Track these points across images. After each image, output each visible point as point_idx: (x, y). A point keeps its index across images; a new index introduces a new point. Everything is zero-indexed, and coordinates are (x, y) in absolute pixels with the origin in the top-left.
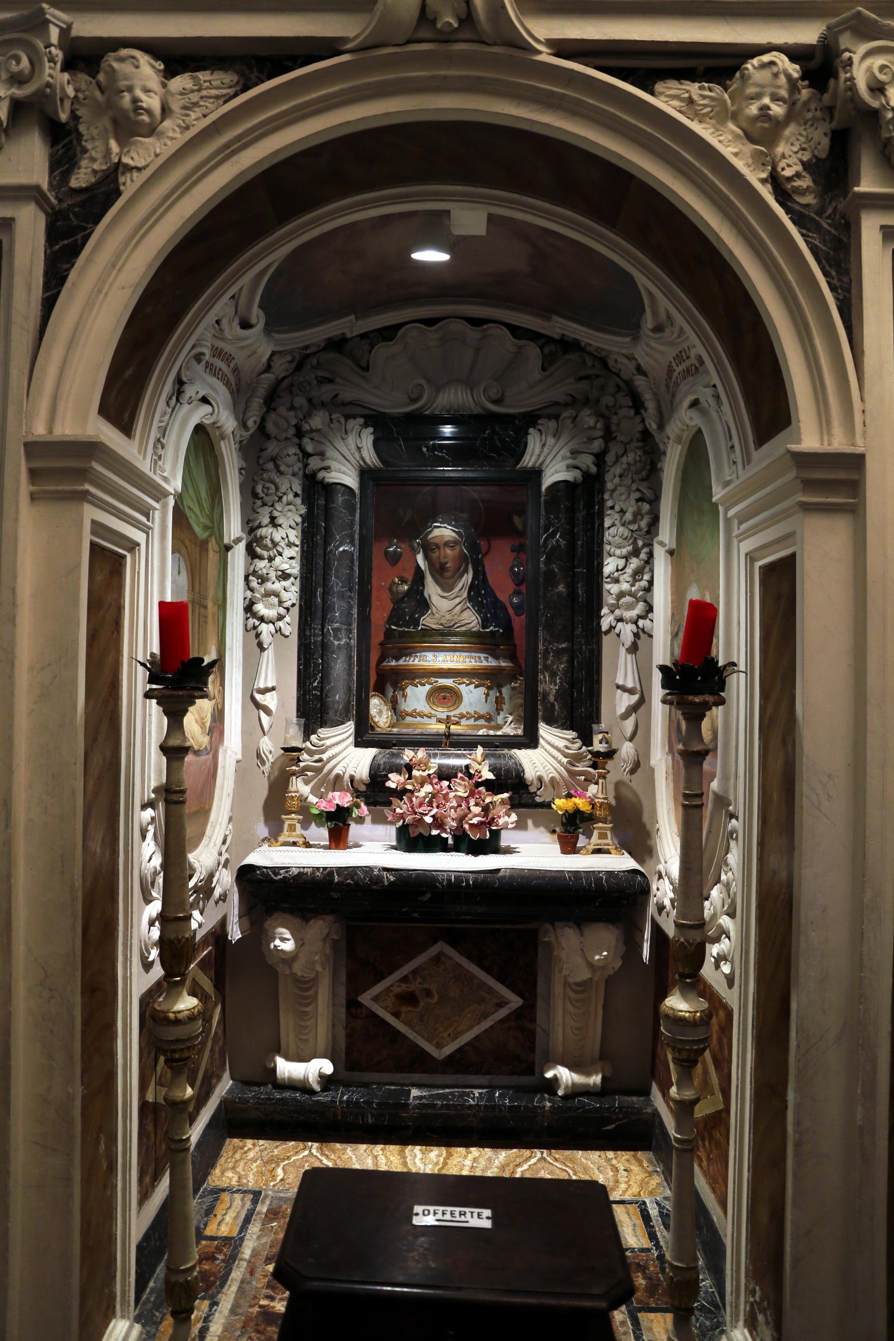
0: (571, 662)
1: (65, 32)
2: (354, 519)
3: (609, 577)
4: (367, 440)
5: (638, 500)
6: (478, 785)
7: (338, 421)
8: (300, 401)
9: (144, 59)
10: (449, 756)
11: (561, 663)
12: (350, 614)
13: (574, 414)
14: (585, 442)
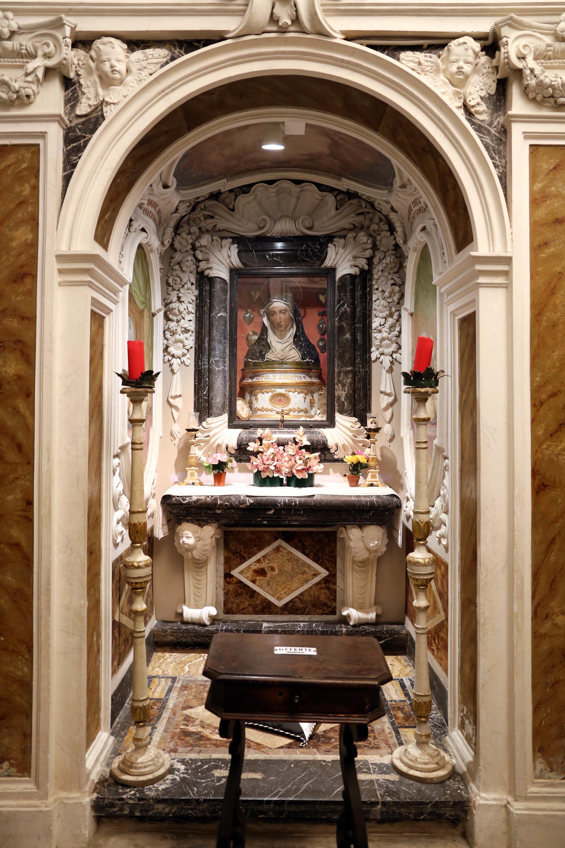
0: (354, 378)
1: (73, 29)
3: (375, 329)
4: (235, 250)
5: (392, 285)
6: (301, 448)
7: (217, 241)
8: (194, 229)
9: (117, 43)
10: (283, 433)
11: (348, 379)
12: (224, 352)
13: (355, 235)
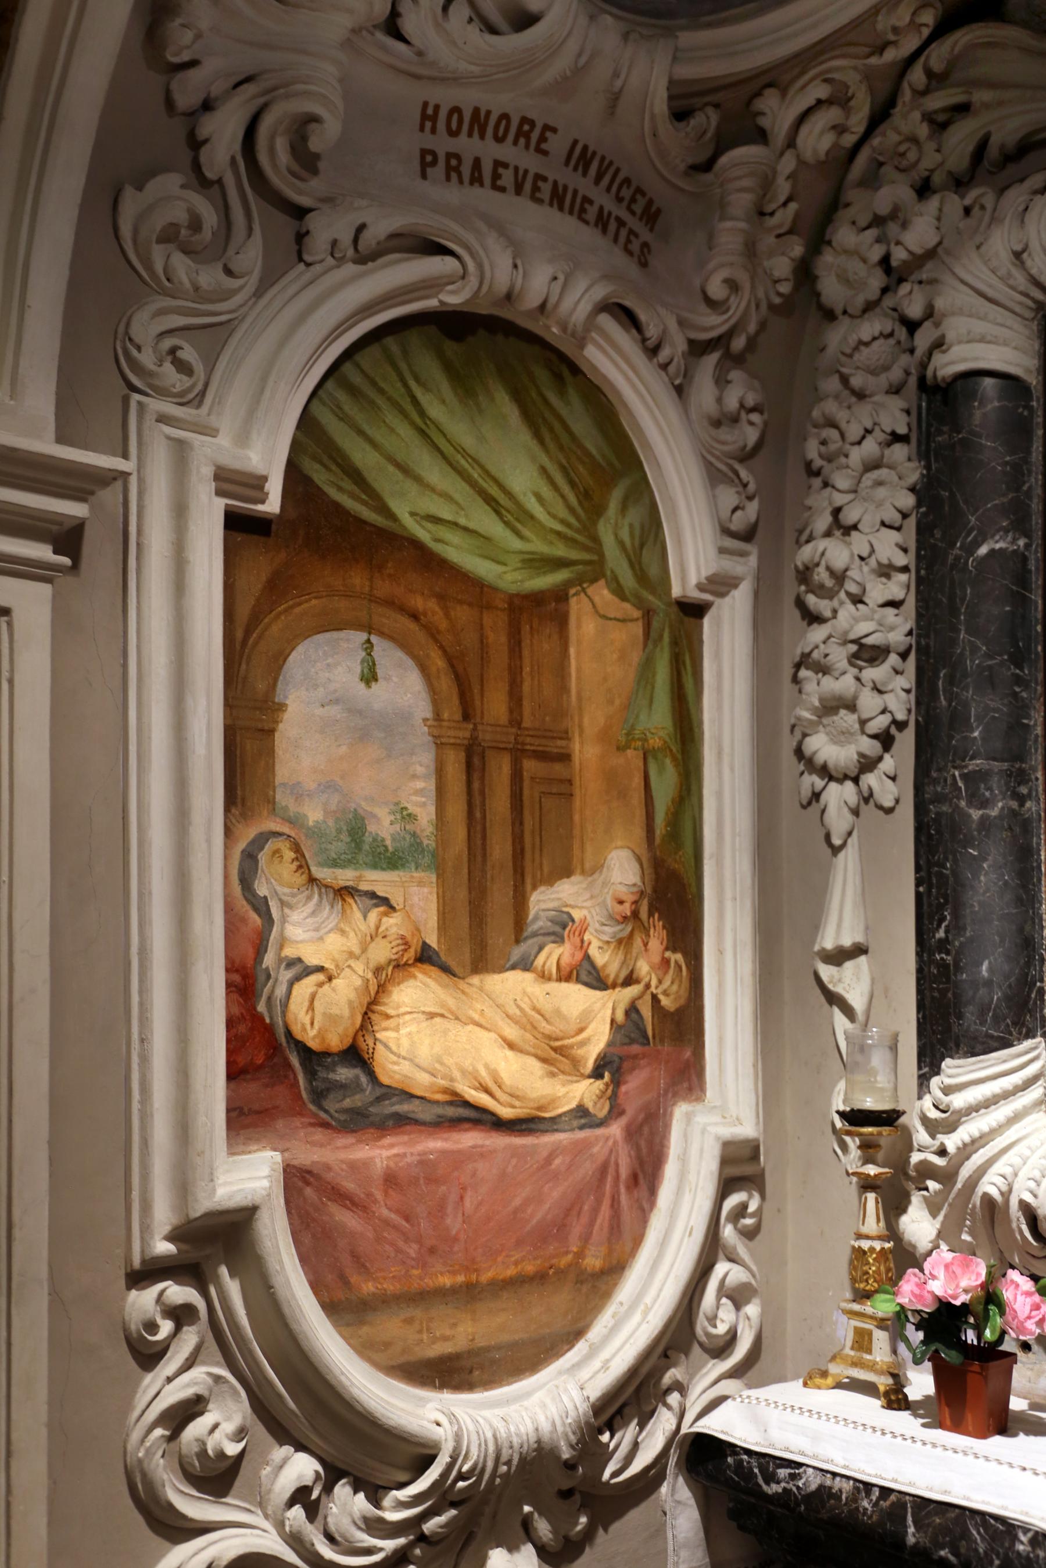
2: (1026, 461)
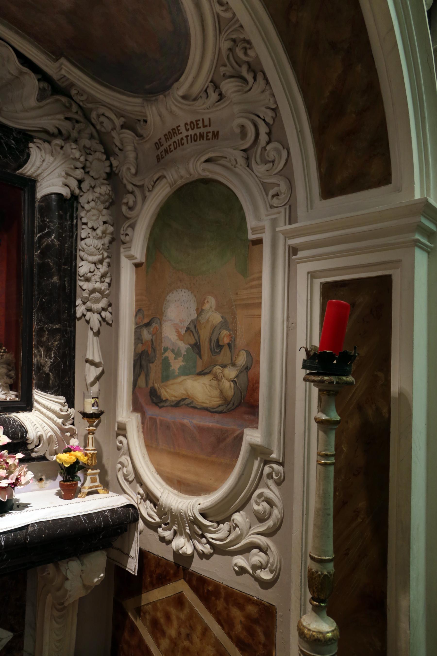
3: (83, 276)
11: (55, 341)
14: (71, 168)
